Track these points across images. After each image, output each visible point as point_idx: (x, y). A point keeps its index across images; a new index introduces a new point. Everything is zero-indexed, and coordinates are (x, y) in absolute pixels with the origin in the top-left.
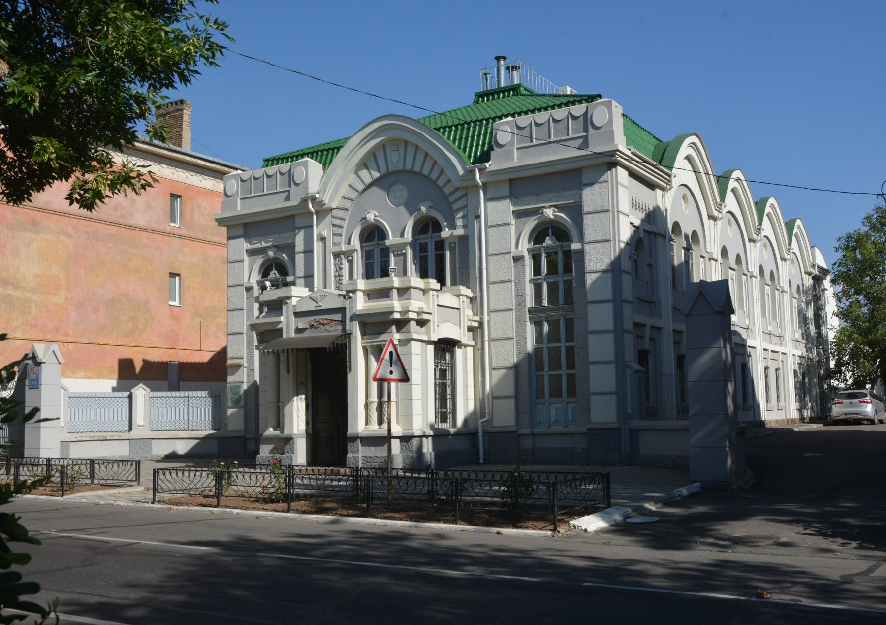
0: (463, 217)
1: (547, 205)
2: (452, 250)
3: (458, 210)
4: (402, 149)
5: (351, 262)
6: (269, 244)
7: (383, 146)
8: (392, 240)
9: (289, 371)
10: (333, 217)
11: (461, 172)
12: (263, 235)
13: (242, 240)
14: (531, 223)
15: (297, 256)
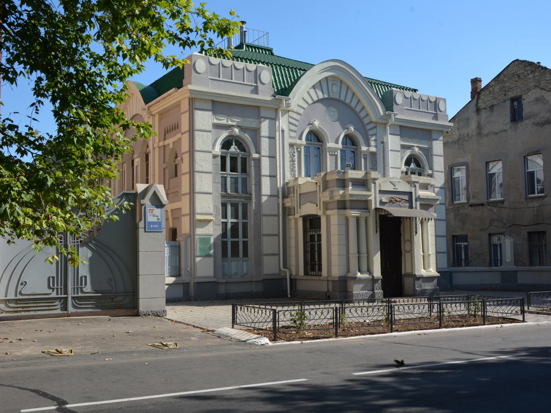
0: (375, 140)
1: (416, 145)
2: (365, 159)
3: (372, 135)
4: (339, 84)
5: (299, 153)
6: (234, 124)
7: (327, 78)
8: (330, 144)
9: (377, 232)
10: (289, 117)
11: (382, 113)
12: (229, 115)
13: (210, 113)
14: (408, 153)
15: (262, 139)
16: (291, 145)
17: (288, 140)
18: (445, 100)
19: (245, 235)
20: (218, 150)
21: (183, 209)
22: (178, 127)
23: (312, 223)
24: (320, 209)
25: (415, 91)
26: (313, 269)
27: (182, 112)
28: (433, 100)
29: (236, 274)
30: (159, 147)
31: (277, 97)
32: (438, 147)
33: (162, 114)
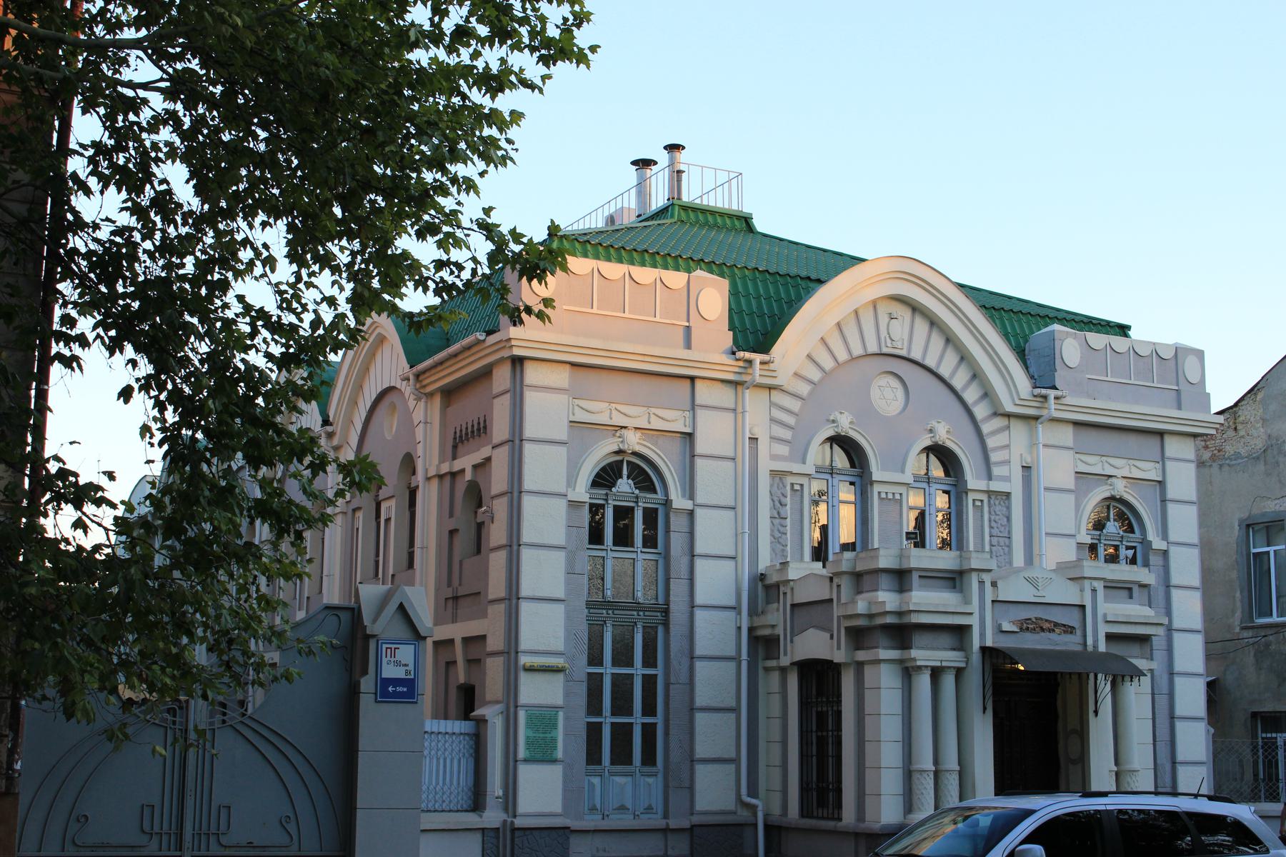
9: (985, 709)
16: (774, 473)
17: (765, 465)
18: (1200, 354)
19: (649, 709)
20: (582, 491)
21: (489, 641)
22: (485, 427)
23: (819, 680)
24: (839, 648)
25: (1123, 330)
26: (822, 803)
27: (496, 390)
28: (1168, 354)
29: (622, 808)
30: (441, 477)
31: (741, 354)
32: (1183, 479)
33: (450, 393)
